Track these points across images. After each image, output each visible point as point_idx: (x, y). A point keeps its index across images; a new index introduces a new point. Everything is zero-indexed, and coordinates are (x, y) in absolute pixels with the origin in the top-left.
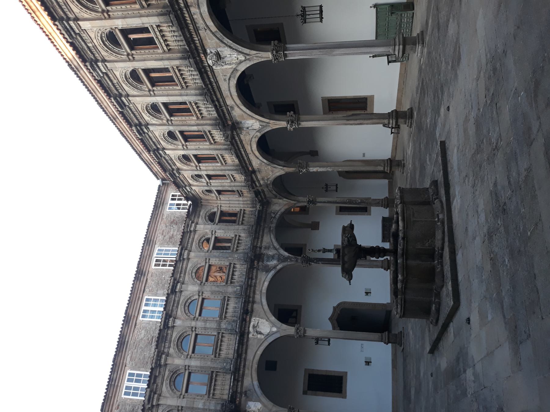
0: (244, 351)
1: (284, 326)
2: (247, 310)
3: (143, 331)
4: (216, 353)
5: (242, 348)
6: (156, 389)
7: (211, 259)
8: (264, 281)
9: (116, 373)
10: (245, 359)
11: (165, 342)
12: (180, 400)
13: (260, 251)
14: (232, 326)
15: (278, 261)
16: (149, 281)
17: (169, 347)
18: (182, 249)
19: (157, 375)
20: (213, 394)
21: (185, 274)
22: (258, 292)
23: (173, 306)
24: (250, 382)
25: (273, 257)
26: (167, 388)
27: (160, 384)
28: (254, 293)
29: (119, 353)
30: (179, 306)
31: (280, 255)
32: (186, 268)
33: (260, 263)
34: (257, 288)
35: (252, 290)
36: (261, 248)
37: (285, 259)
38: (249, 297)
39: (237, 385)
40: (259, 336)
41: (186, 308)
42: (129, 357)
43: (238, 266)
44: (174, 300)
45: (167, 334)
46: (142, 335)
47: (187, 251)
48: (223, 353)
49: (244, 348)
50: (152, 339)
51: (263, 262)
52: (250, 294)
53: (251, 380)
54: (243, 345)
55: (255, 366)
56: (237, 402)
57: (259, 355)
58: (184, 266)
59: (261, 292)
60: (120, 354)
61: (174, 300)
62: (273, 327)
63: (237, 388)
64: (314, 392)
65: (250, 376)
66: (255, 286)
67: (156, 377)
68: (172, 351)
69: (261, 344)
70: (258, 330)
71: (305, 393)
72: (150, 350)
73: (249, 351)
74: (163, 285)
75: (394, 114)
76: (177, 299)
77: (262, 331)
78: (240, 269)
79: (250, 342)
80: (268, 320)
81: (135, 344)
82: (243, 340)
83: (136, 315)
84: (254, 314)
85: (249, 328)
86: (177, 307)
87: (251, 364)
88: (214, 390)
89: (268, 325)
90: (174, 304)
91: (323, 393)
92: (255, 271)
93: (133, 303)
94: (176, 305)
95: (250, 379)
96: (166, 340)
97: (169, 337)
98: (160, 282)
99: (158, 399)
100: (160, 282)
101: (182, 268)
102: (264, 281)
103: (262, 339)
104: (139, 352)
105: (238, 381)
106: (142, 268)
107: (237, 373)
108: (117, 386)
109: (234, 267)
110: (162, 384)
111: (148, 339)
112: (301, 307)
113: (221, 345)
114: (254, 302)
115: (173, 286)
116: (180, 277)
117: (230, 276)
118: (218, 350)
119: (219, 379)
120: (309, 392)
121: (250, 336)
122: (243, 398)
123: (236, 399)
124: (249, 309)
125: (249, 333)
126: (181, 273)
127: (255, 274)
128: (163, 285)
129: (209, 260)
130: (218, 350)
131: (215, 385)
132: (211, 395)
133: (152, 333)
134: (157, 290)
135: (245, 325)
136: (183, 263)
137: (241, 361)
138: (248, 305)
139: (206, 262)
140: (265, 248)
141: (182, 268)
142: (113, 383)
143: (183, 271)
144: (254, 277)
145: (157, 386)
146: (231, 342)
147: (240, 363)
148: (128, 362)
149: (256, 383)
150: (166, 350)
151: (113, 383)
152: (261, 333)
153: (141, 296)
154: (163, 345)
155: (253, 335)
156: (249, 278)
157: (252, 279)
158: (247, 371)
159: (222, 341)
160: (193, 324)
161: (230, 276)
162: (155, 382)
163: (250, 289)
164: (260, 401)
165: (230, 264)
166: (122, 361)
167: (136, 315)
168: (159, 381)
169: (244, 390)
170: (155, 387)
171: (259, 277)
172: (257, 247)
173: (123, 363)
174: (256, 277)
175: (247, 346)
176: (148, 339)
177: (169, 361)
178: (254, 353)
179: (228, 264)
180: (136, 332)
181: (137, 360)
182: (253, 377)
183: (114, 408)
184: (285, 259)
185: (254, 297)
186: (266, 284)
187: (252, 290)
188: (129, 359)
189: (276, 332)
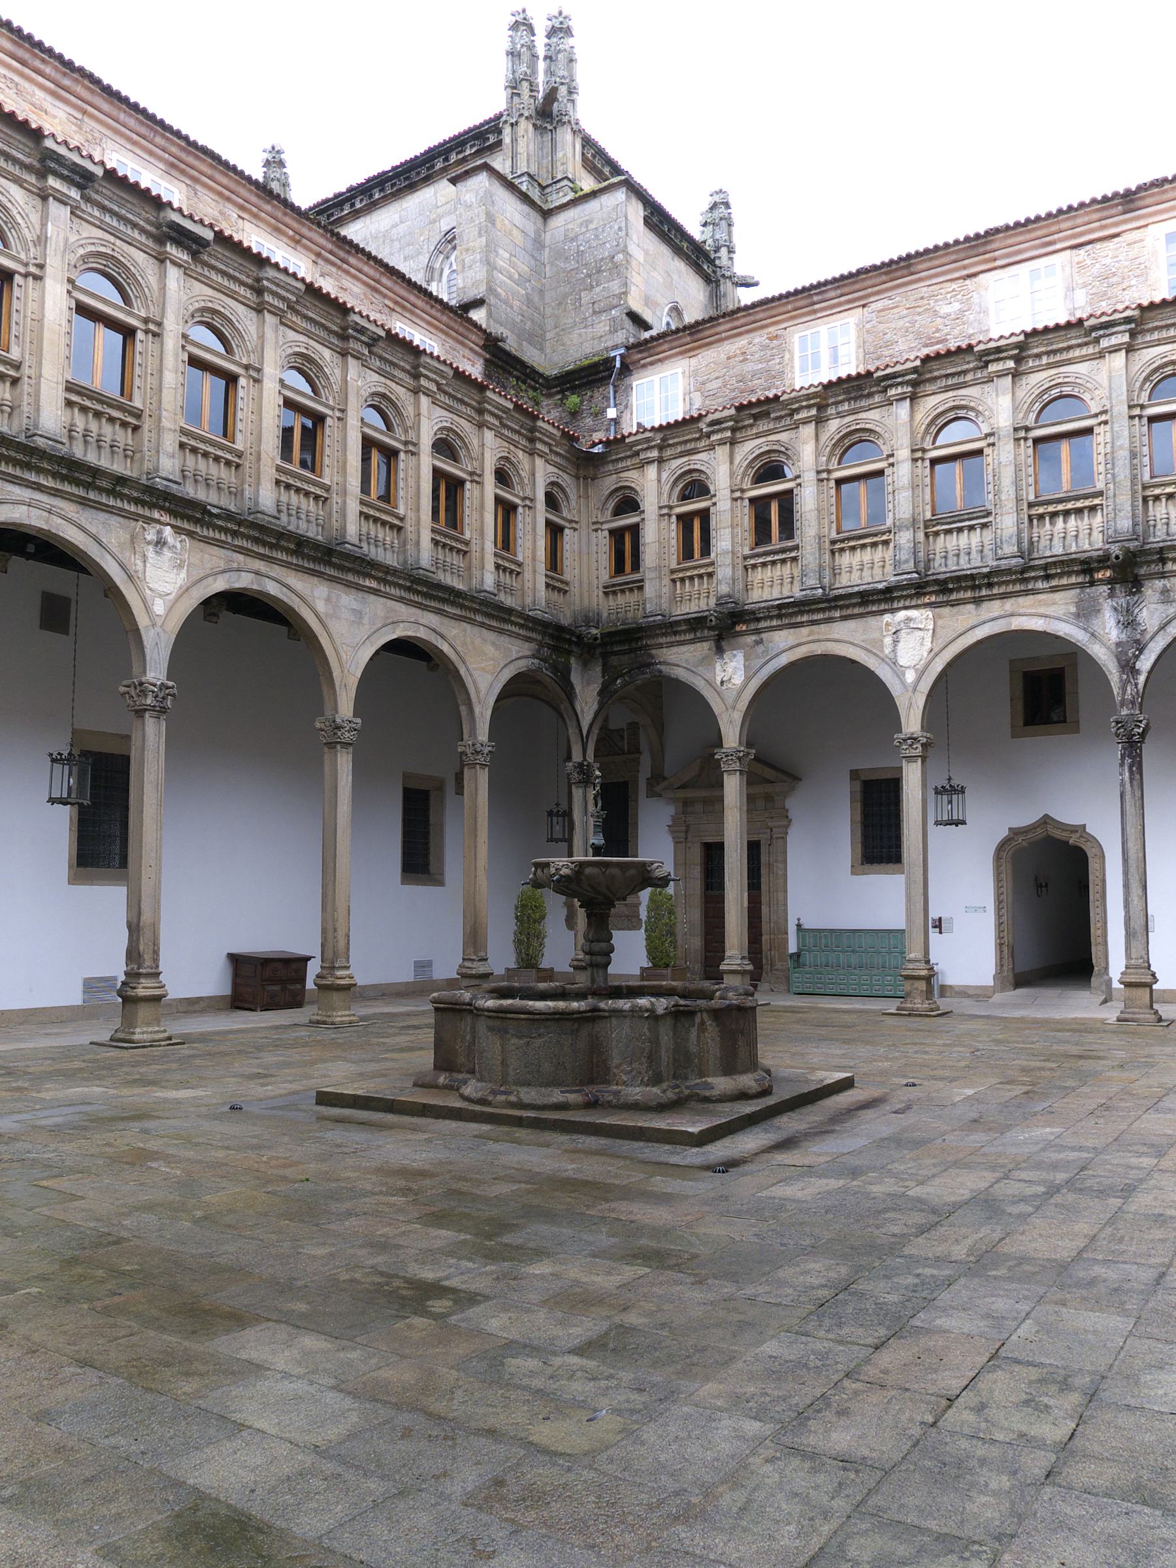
0: (849, 612)
1: (920, 701)
2: (951, 591)
3: (956, 306)
4: (842, 541)
5: (854, 605)
6: (744, 427)
7: (1108, 427)
8: (1046, 614)
9: (839, 292)
10: (830, 620)
11: (849, 400)
12: (727, 492)
13: (1152, 576)
14: (907, 561)
15: (1118, 644)
16: (1112, 244)
17: (840, 415)
18: (1128, 320)
19: (772, 416)
20: (754, 566)
21: (1050, 366)
22: (1009, 605)
23: (947, 376)
24: (783, 646)
25: (1129, 622)
26: (751, 451)
27: (755, 431)
28: (1004, 596)
29: (886, 273)
30: (951, 394)
31: (1141, 647)
32: (1070, 362)
33: (1104, 589)
34: (1021, 600)
35: (1010, 588)
36: (1163, 575)
37: (1128, 668)
38: (990, 585)
39: (771, 618)
40: (888, 640)
41: (951, 415)
42: (887, 302)
43: (1098, 519)
44: (965, 372)
45: (870, 395)
46: (945, 309)
47: (1126, 338)
48: (845, 560)
49: (856, 611)
50: (937, 343)
51: (1111, 596)
52: (1000, 584)
53: (787, 645)
54: (860, 605)
55: (818, 649)
56: (738, 628)
57: (843, 654)
58: (1077, 353)
59: (1012, 615)
60: (884, 278)
61: (965, 372)
62: (916, 671)
63: (765, 618)
64: (858, 796)
65: (797, 642)
66: (1027, 593)
67: (766, 415)
68: (834, 425)
69: (870, 651)
70: (903, 634)
71: (854, 775)
72: (911, 349)
73: (851, 624)
74: (1103, 296)
75: (157, 992)
76: (969, 377)
77: (900, 646)
78: (1084, 535)
79: (872, 621)
80: (934, 654)
81: (921, 303)
82: (873, 602)
83: (998, 263)
84: (946, 611)
85: (906, 608)
86: (948, 389)
87: (821, 637)
88: (764, 564)
89: (917, 658)
90: (953, 375)
91: (858, 818)
92: (1073, 579)
93: (1028, 236)
94: (950, 382)
95: (792, 641)
96: (855, 399)
97: (864, 403)
98: (1114, 280)
99: (722, 443)
100: (1114, 280)
101: (1070, 348)
102: (1041, 616)
103: (882, 651)
104: (901, 323)
105: (779, 616)
106: (1148, 201)
107: (791, 612)
108: (815, 312)
109: (1093, 509)
110: (758, 436)
111: (938, 330)
112: (1076, 729)
113: (864, 546)
114: (977, 601)
115: (998, 350)
116: (1038, 356)
117: (1060, 507)
118: (852, 543)
119: (787, 569)
120: (858, 787)
121: (887, 617)
122: (750, 639)
123: (745, 622)
124: (954, 596)
125: (893, 611)
126: (1048, 353)
127: (1064, 581)
128: (1103, 296)
129: (1106, 423)
130: (852, 543)
131: (774, 563)
132: (752, 562)
133: (956, 332)
134: (1085, 285)
135: (911, 597)
136: (1086, 344)
137: (823, 610)
138: (965, 589)
139: (1096, 415)
140: (1165, 591)
141: (1070, 348)
142: (815, 298)
143: (1058, 358)
144: (1054, 583)
145: (751, 426)
146: (877, 571)
147: (819, 610)
148: (873, 306)
149: (784, 660)
150: (831, 411)
151: (815, 298)
152: (896, 642)
153: (1058, 246)
154: (840, 398)
155: (888, 624)
156: (1046, 567)
157: (1048, 577)
158: (804, 631)
159: (874, 545)
160: (904, 454)
161: (1060, 507)
162: (756, 417)
163: (1014, 582)
164: (748, 679)
165: (1100, 494)
166: (870, 290)
167: (998, 263)
168: (763, 426)
169: (764, 636)
170: (746, 423)
171: (1058, 596)
172: (1163, 561)
173: (869, 296)
174: (1054, 589)
175: (861, 616)
176: (938, 330)
177: (808, 431)
178: (845, 638)
179: (1100, 486)
180: (954, 286)
181: (881, 327)
182: (795, 650)
183: (771, 329)
184: (1128, 668)
185: (991, 598)
186: (1037, 624)
187: (1010, 588)
188: (879, 305)
189: (903, 682)
